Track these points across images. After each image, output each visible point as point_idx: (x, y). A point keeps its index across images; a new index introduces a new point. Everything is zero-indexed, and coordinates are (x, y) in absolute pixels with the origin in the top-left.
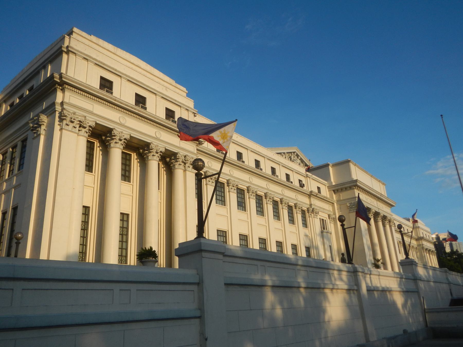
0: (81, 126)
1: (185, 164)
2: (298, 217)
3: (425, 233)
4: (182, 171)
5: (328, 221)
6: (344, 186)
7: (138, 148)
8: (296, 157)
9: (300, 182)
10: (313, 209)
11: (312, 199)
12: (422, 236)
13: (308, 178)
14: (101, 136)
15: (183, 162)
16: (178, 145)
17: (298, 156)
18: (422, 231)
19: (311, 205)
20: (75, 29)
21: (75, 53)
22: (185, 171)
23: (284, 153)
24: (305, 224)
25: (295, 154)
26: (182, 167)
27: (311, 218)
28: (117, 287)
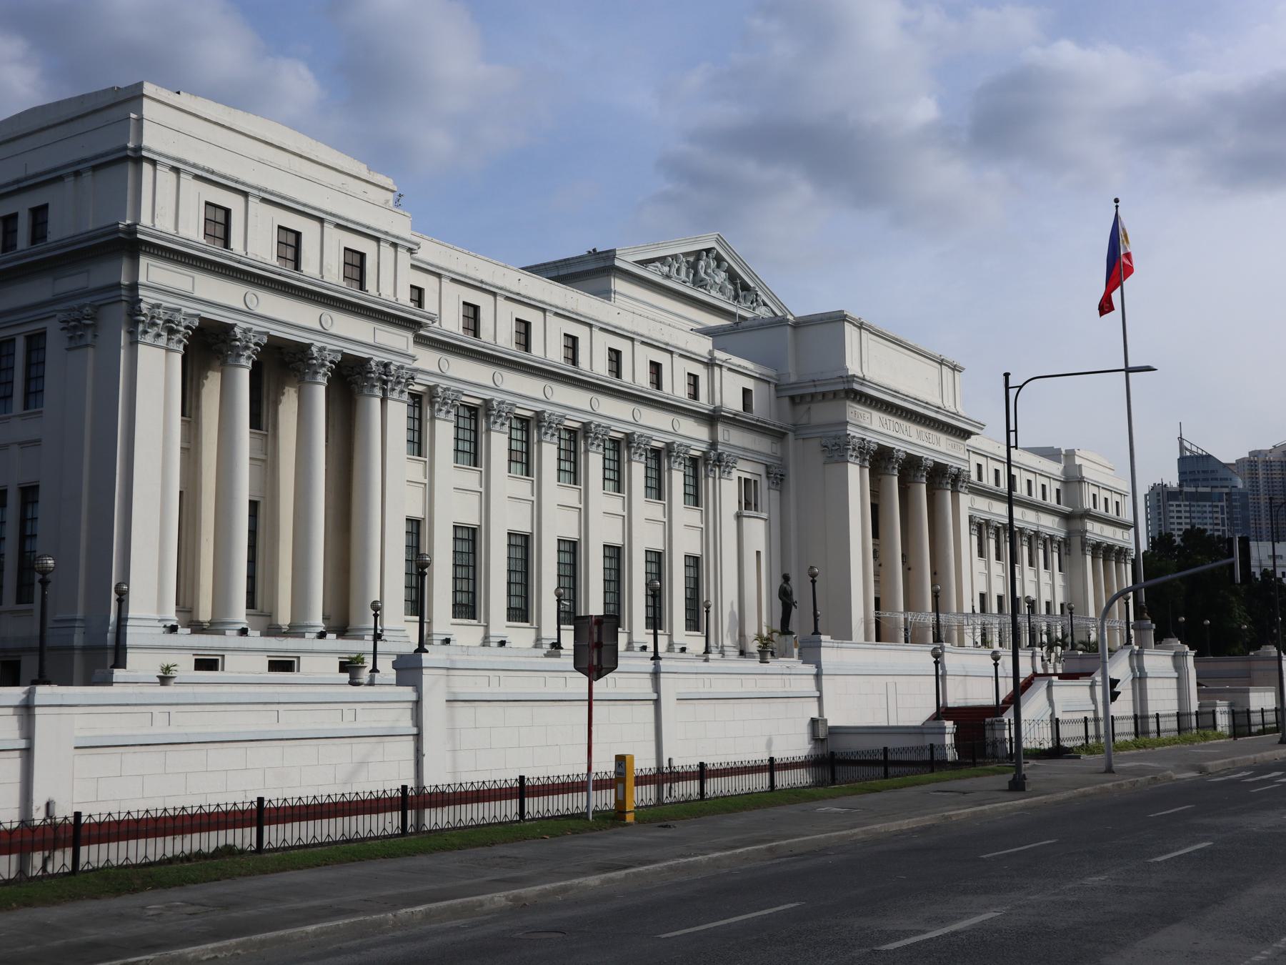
0: (171, 332)
1: (385, 382)
5: (764, 484)
6: (820, 389)
7: (281, 363)
8: (713, 264)
10: (720, 454)
11: (720, 428)
12: (1088, 504)
13: (717, 370)
15: (380, 379)
16: (371, 341)
17: (719, 259)
18: (1094, 490)
20: (149, 89)
21: (154, 163)
23: (675, 257)
24: (694, 497)
26: (378, 392)
27: (710, 480)
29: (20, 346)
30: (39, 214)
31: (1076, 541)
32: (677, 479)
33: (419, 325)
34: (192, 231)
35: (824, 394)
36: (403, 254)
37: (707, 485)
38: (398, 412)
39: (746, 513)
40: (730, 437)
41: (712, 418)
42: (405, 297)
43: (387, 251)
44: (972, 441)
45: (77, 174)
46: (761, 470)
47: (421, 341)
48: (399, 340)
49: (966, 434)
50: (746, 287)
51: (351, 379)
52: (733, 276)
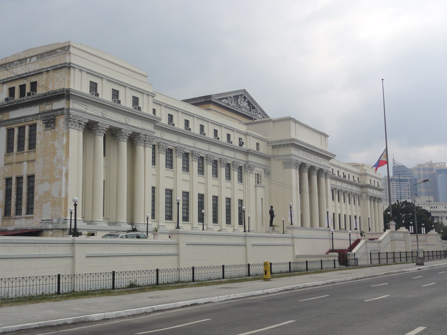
0: (80, 124)
2: (235, 174)
3: (373, 179)
4: (143, 147)
5: (263, 175)
7: (113, 133)
8: (243, 100)
9: (240, 140)
12: (368, 183)
14: (90, 128)
16: (141, 127)
17: (245, 98)
18: (370, 178)
19: (247, 162)
21: (74, 68)
22: (145, 147)
23: (230, 97)
24: (241, 180)
25: (243, 96)
28: (158, 246)
29: (27, 128)
30: (34, 85)
31: (364, 196)
32: (235, 174)
33: (156, 121)
34: (86, 90)
35: (284, 145)
36: (150, 98)
37: (245, 176)
38: (149, 151)
39: (258, 185)
40: (252, 159)
41: (247, 153)
42: (151, 113)
43: (145, 96)
44: (331, 161)
45: (48, 71)
46: (262, 170)
47: (156, 127)
48: (149, 127)
49: (329, 158)
50: (254, 108)
51: (133, 140)
52: (249, 104)
